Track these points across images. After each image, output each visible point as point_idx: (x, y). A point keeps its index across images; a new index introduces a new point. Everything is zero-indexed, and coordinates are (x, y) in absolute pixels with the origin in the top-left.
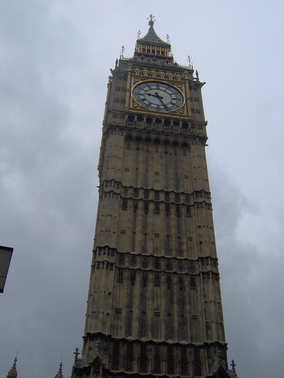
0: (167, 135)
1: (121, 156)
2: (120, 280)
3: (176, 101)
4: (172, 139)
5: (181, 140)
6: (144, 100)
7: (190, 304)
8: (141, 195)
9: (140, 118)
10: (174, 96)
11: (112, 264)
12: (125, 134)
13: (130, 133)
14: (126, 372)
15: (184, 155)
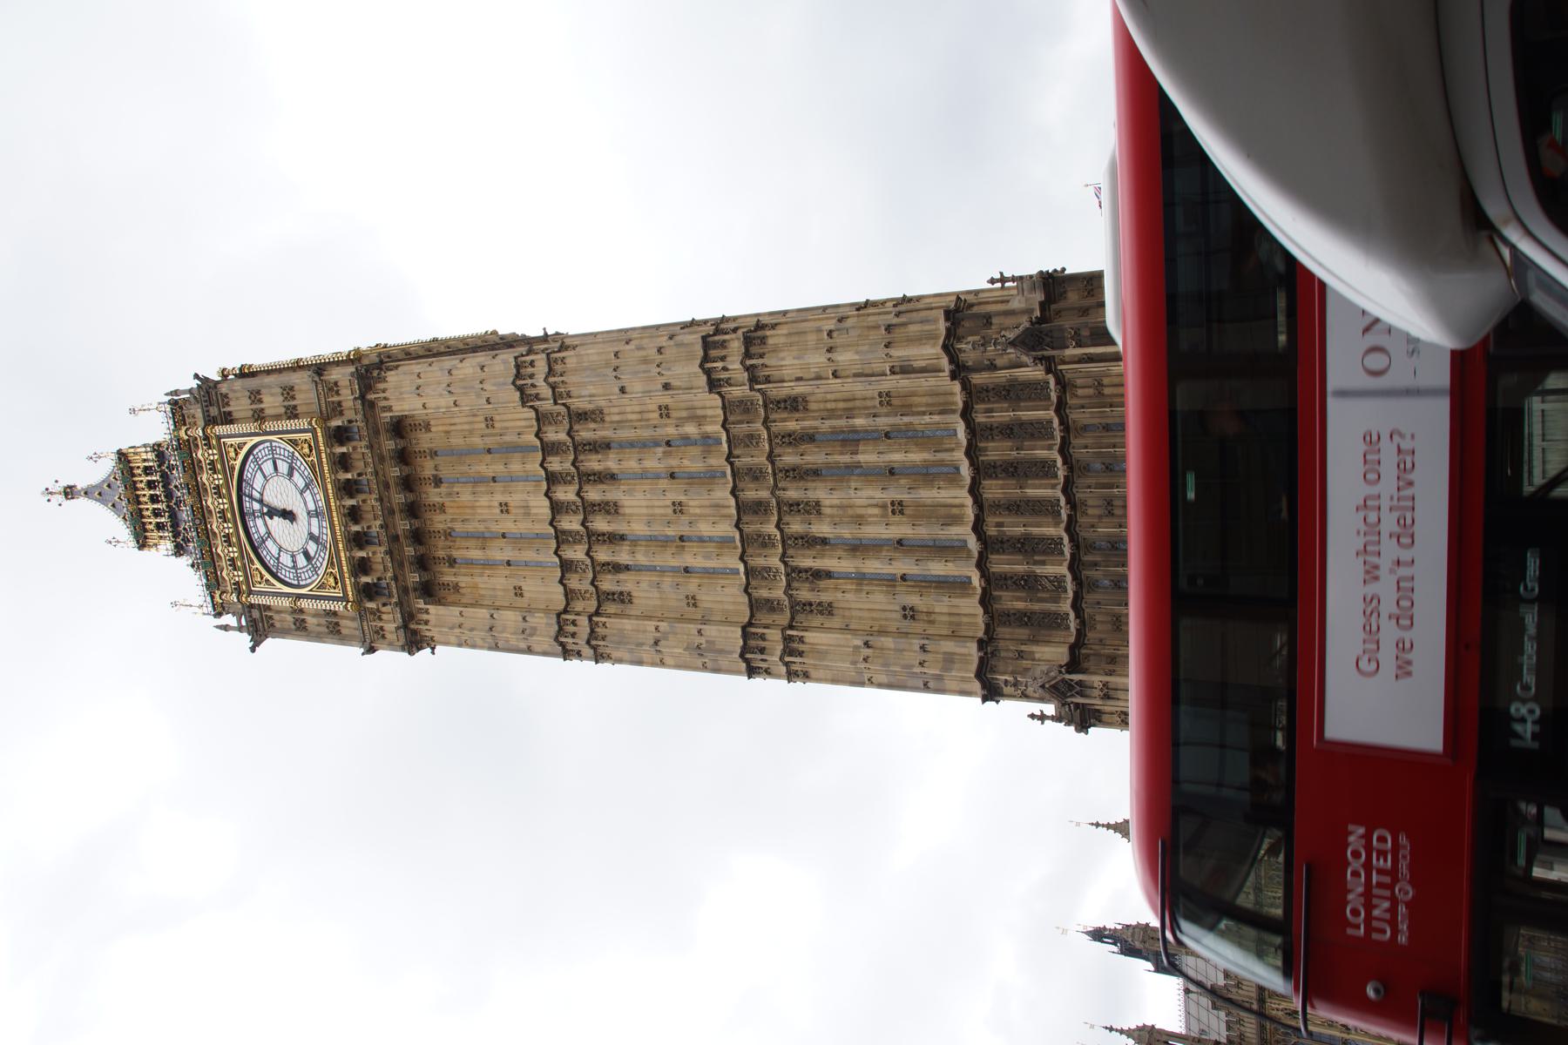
0: (387, 486)
1: (483, 613)
2: (828, 610)
3: (279, 463)
4: (395, 472)
5: (389, 445)
6: (306, 554)
7: (850, 413)
8: (576, 553)
9: (362, 567)
10: (268, 467)
11: (787, 640)
12: (421, 604)
13: (415, 590)
14: (1071, 594)
15: (427, 427)
